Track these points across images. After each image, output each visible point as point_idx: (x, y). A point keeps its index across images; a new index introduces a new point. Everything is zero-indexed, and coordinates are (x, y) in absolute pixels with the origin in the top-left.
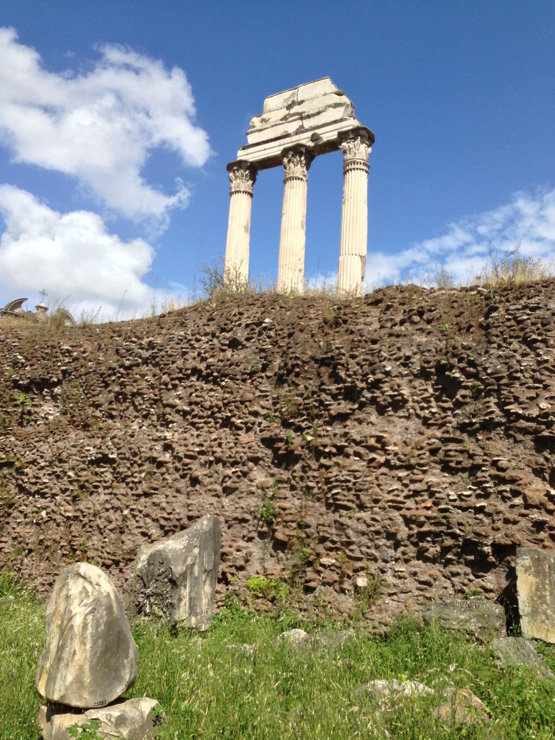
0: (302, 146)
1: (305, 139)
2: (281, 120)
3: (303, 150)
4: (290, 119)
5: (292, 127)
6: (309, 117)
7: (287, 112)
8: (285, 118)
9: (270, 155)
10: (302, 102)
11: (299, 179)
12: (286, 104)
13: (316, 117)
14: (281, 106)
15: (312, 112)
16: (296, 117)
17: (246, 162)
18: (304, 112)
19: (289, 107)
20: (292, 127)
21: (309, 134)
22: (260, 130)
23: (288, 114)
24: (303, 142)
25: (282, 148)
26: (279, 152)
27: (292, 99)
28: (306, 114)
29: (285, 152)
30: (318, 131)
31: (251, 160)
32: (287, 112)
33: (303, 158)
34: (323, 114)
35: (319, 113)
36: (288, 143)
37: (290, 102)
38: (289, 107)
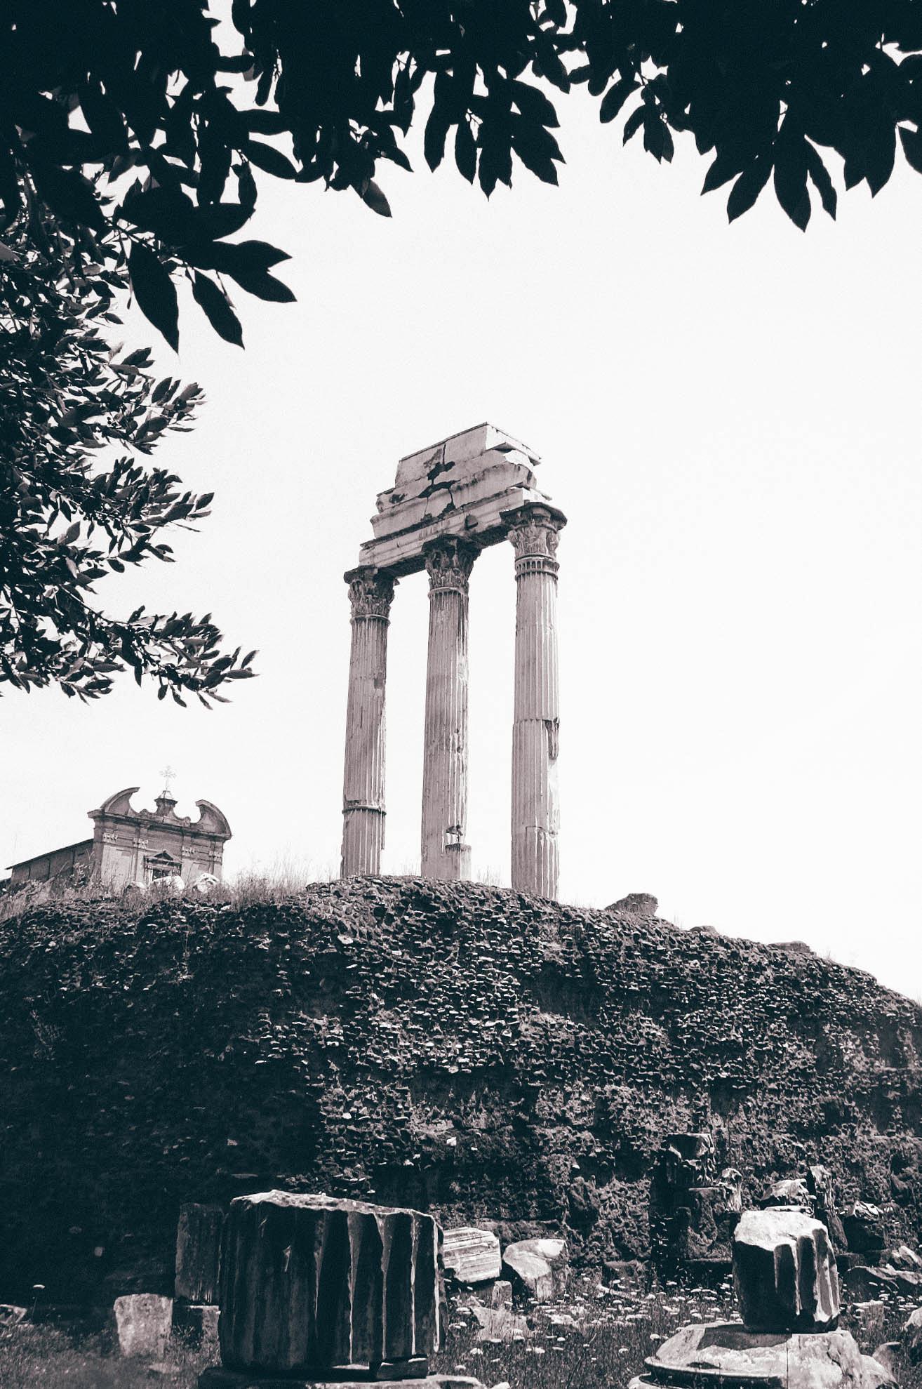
0: (452, 537)
1: (455, 525)
2: (420, 496)
3: (454, 543)
4: (433, 495)
6: (460, 488)
8: (426, 494)
11: (451, 592)
14: (419, 474)
15: (464, 482)
16: (443, 490)
17: (371, 568)
18: (454, 482)
19: (432, 476)
20: (437, 505)
21: (462, 517)
22: (392, 515)
24: (452, 531)
25: (423, 542)
27: (436, 461)
29: (428, 547)
30: (475, 512)
31: (379, 565)
33: (455, 558)
34: (481, 484)
35: (474, 482)
36: (430, 533)
37: (433, 467)
38: (432, 476)
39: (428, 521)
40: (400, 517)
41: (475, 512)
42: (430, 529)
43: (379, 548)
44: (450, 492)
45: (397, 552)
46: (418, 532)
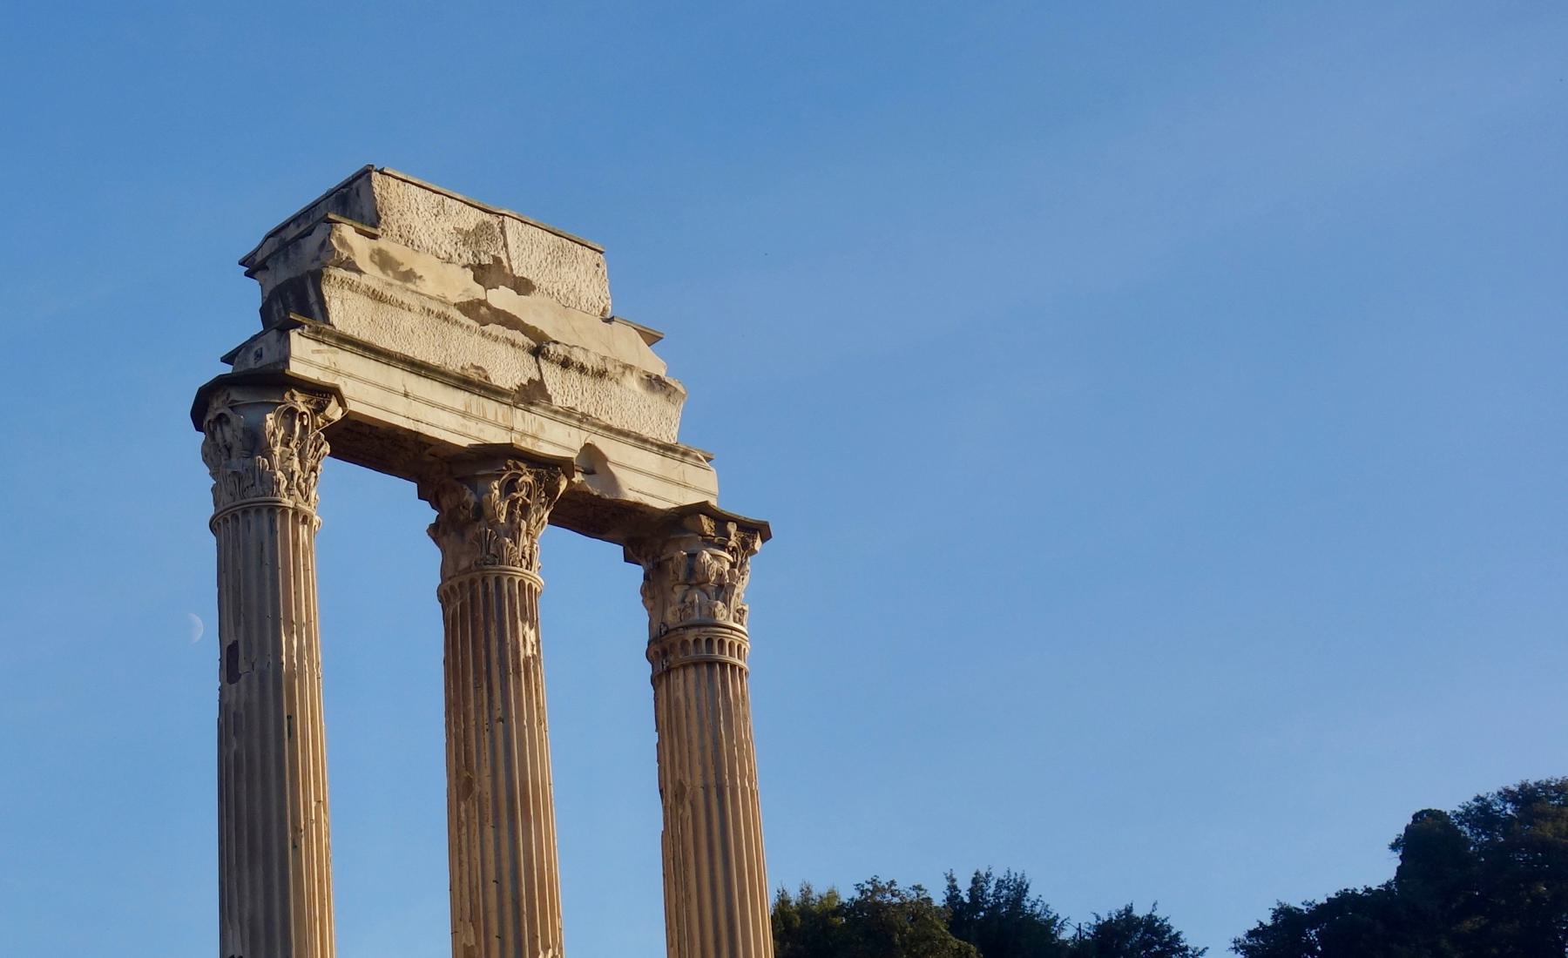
4: (492, 328)
5: (510, 368)
6: (566, 364)
7: (478, 291)
8: (471, 308)
9: (423, 429)
10: (523, 286)
12: (468, 257)
13: (588, 382)
15: (578, 356)
16: (520, 338)
17: (342, 402)
23: (482, 303)
26: (464, 442)
28: (561, 350)
31: (353, 406)
32: (478, 291)
35: (601, 374)
37: (486, 260)
39: (473, 384)
40: (408, 320)
41: (612, 450)
42: (491, 407)
43: (348, 361)
44: (538, 352)
45: (399, 404)
46: (459, 399)
